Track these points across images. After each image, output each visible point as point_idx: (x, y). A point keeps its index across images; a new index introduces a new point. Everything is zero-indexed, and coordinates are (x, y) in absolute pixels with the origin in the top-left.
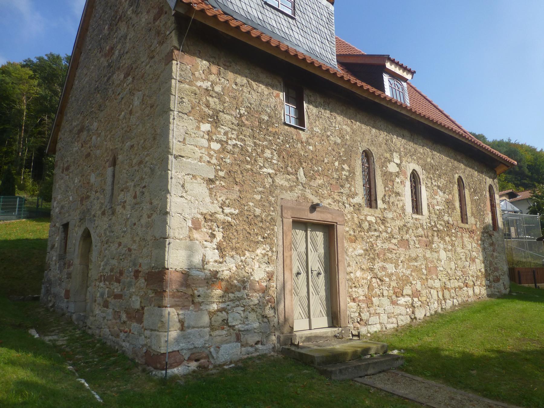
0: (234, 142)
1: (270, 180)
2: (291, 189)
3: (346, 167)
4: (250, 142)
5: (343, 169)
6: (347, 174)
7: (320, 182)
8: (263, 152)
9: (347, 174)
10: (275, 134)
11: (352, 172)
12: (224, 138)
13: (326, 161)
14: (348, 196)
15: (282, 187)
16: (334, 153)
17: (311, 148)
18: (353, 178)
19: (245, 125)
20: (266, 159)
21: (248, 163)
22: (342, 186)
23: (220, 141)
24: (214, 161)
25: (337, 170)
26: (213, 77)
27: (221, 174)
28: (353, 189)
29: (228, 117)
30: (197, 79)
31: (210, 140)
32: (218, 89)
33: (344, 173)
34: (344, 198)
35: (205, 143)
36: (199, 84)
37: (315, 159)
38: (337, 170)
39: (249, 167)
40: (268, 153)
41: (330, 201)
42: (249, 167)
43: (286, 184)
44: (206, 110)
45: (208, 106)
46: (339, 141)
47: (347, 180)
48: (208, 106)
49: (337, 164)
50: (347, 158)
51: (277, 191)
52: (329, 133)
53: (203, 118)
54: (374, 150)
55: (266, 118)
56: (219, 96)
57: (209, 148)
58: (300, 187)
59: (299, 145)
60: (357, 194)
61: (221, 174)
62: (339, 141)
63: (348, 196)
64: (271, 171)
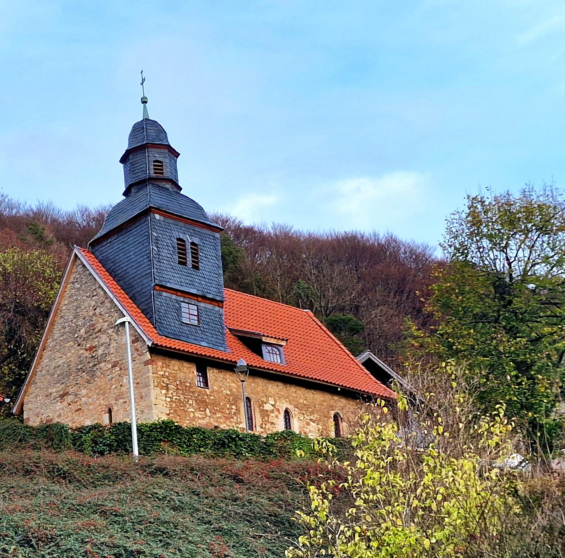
0: (175, 397)
1: (192, 414)
2: (203, 418)
3: (234, 407)
4: (182, 397)
5: (232, 408)
6: (235, 411)
7: (219, 415)
8: (188, 401)
9: (235, 411)
10: (193, 392)
11: (238, 410)
12: (171, 396)
13: (221, 404)
14: (236, 423)
15: (199, 418)
16: (226, 400)
17: (212, 398)
18: (239, 413)
19: (179, 389)
20: (190, 404)
21: (182, 406)
22: (232, 418)
23: (170, 397)
24: (168, 406)
25: (228, 409)
26: (164, 369)
27: (172, 411)
28: (239, 420)
29: (172, 386)
30: (159, 371)
31: (166, 397)
32: (167, 374)
33: (233, 410)
34: (234, 424)
35: (164, 398)
36: (159, 373)
37: (215, 403)
38: (228, 409)
39: (182, 408)
40: (191, 402)
41: (225, 425)
42: (182, 408)
43: (200, 416)
44: (163, 384)
45: (163, 382)
46: (229, 393)
47: (235, 414)
48: (163, 382)
49: (228, 406)
50: (235, 402)
51: (196, 420)
52: (222, 389)
53: (162, 388)
54: (251, 396)
55: (188, 385)
56: (167, 377)
57: (166, 400)
58: (208, 418)
59: (206, 397)
60: (241, 423)
61: (172, 411)
62: (229, 393)
63: (236, 423)
64: (193, 410)
